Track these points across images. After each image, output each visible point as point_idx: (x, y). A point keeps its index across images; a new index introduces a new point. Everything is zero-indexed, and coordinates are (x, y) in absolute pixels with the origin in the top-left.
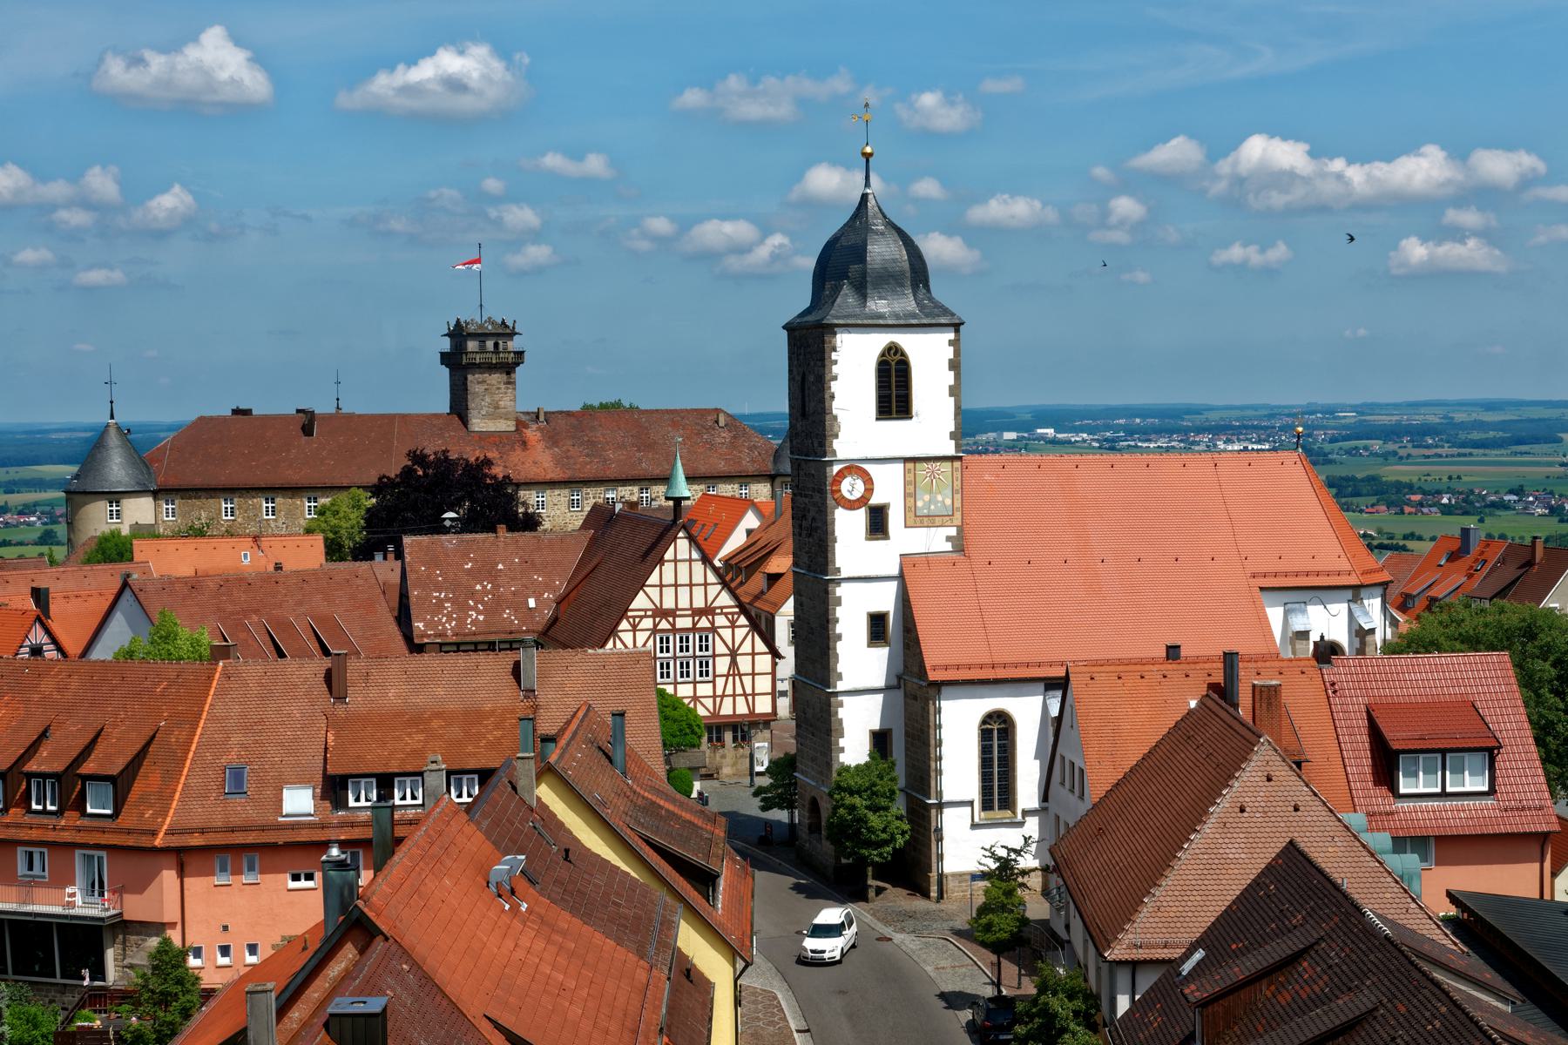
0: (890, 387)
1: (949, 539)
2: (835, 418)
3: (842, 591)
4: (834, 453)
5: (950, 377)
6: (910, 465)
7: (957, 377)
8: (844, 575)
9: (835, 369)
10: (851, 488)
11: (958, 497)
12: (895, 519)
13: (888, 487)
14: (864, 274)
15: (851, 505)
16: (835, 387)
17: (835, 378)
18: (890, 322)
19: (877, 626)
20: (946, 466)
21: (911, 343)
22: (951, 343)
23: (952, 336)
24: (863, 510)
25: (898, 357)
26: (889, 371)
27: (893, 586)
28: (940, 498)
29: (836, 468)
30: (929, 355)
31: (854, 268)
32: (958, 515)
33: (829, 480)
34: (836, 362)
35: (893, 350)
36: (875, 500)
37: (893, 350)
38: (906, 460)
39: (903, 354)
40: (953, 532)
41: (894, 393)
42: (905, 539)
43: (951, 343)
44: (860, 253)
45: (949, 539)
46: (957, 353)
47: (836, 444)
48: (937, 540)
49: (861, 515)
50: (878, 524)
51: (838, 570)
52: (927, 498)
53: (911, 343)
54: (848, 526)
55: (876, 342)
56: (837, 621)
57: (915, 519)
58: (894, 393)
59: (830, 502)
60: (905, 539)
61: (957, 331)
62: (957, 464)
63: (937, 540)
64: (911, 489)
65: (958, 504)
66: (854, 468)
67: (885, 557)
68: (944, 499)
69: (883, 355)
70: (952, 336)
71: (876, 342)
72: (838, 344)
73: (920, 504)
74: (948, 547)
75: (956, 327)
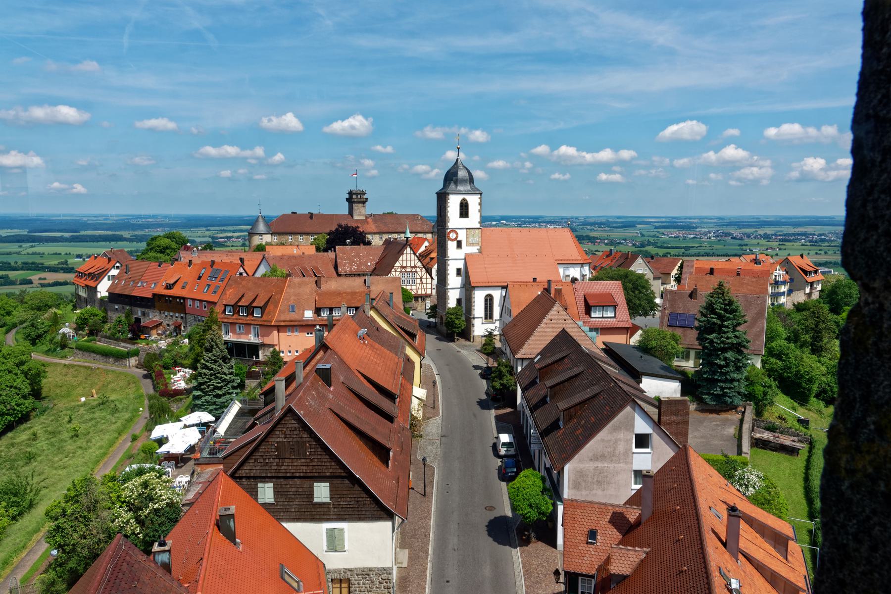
12: (464, 244)
13: (462, 235)
15: (452, 240)
16: (449, 209)
21: (468, 197)
30: (473, 201)
35: (464, 200)
36: (459, 239)
37: (464, 200)
44: (456, 174)
49: (455, 243)
50: (459, 245)
53: (468, 197)
54: (451, 246)
55: (460, 197)
57: (469, 244)
60: (466, 249)
63: (474, 250)
66: (453, 231)
67: (461, 254)
71: (460, 197)
75: (481, 194)
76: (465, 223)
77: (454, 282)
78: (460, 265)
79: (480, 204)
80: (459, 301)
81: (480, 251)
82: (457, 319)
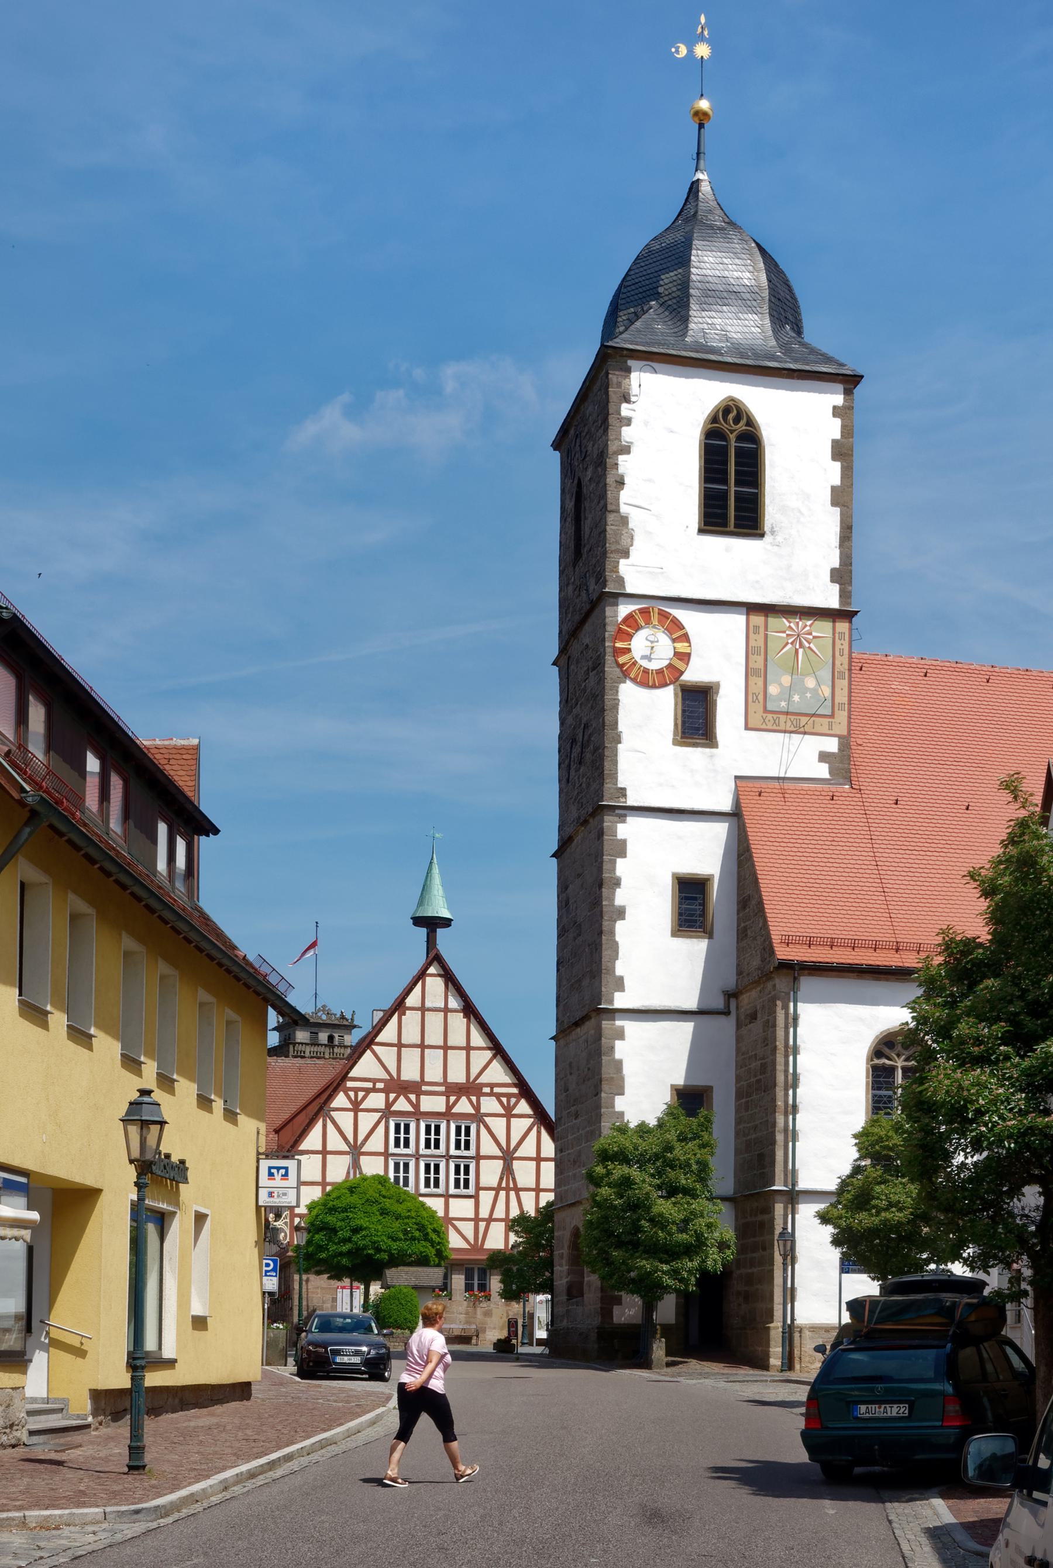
0: (725, 481)
1: (824, 757)
2: (624, 520)
3: (628, 829)
4: (621, 581)
5: (833, 473)
6: (758, 620)
7: (847, 472)
8: (630, 802)
9: (627, 434)
10: (649, 647)
11: (843, 684)
12: (729, 711)
13: (718, 651)
14: (685, 284)
15: (649, 680)
16: (625, 464)
17: (626, 450)
18: (729, 360)
19: (690, 897)
20: (823, 629)
21: (770, 406)
22: (836, 411)
23: (839, 399)
24: (671, 688)
25: (742, 426)
26: (724, 451)
27: (720, 830)
28: (810, 683)
29: (624, 610)
30: (797, 427)
31: (668, 280)
32: (842, 716)
33: (611, 630)
34: (628, 422)
36: (694, 674)
38: (752, 608)
39: (751, 422)
40: (832, 745)
41: (732, 487)
42: (743, 749)
43: (836, 411)
45: (824, 757)
46: (847, 431)
47: (625, 567)
48: (804, 757)
51: (623, 792)
52: (786, 680)
53: (770, 406)
56: (617, 883)
58: (732, 487)
59: (611, 670)
60: (743, 749)
61: (848, 392)
62: (842, 626)
63: (804, 757)
64: (758, 662)
65: (842, 697)
66: (660, 611)
67: (704, 778)
68: (816, 686)
69: (714, 419)
70: (839, 399)
72: (634, 389)
73: (773, 690)
74: (823, 771)
75: (850, 382)
76: (733, 565)
77: (656, 963)
78: (704, 852)
79: (841, 451)
80: (690, 1099)
81: (842, 764)
82: (672, 1191)
